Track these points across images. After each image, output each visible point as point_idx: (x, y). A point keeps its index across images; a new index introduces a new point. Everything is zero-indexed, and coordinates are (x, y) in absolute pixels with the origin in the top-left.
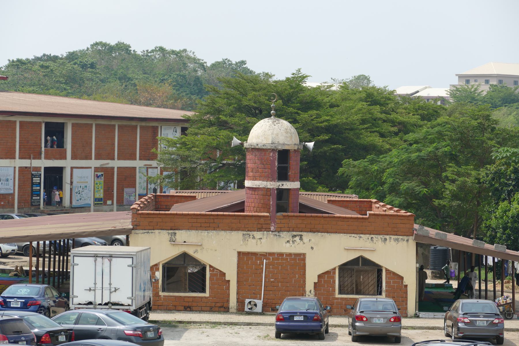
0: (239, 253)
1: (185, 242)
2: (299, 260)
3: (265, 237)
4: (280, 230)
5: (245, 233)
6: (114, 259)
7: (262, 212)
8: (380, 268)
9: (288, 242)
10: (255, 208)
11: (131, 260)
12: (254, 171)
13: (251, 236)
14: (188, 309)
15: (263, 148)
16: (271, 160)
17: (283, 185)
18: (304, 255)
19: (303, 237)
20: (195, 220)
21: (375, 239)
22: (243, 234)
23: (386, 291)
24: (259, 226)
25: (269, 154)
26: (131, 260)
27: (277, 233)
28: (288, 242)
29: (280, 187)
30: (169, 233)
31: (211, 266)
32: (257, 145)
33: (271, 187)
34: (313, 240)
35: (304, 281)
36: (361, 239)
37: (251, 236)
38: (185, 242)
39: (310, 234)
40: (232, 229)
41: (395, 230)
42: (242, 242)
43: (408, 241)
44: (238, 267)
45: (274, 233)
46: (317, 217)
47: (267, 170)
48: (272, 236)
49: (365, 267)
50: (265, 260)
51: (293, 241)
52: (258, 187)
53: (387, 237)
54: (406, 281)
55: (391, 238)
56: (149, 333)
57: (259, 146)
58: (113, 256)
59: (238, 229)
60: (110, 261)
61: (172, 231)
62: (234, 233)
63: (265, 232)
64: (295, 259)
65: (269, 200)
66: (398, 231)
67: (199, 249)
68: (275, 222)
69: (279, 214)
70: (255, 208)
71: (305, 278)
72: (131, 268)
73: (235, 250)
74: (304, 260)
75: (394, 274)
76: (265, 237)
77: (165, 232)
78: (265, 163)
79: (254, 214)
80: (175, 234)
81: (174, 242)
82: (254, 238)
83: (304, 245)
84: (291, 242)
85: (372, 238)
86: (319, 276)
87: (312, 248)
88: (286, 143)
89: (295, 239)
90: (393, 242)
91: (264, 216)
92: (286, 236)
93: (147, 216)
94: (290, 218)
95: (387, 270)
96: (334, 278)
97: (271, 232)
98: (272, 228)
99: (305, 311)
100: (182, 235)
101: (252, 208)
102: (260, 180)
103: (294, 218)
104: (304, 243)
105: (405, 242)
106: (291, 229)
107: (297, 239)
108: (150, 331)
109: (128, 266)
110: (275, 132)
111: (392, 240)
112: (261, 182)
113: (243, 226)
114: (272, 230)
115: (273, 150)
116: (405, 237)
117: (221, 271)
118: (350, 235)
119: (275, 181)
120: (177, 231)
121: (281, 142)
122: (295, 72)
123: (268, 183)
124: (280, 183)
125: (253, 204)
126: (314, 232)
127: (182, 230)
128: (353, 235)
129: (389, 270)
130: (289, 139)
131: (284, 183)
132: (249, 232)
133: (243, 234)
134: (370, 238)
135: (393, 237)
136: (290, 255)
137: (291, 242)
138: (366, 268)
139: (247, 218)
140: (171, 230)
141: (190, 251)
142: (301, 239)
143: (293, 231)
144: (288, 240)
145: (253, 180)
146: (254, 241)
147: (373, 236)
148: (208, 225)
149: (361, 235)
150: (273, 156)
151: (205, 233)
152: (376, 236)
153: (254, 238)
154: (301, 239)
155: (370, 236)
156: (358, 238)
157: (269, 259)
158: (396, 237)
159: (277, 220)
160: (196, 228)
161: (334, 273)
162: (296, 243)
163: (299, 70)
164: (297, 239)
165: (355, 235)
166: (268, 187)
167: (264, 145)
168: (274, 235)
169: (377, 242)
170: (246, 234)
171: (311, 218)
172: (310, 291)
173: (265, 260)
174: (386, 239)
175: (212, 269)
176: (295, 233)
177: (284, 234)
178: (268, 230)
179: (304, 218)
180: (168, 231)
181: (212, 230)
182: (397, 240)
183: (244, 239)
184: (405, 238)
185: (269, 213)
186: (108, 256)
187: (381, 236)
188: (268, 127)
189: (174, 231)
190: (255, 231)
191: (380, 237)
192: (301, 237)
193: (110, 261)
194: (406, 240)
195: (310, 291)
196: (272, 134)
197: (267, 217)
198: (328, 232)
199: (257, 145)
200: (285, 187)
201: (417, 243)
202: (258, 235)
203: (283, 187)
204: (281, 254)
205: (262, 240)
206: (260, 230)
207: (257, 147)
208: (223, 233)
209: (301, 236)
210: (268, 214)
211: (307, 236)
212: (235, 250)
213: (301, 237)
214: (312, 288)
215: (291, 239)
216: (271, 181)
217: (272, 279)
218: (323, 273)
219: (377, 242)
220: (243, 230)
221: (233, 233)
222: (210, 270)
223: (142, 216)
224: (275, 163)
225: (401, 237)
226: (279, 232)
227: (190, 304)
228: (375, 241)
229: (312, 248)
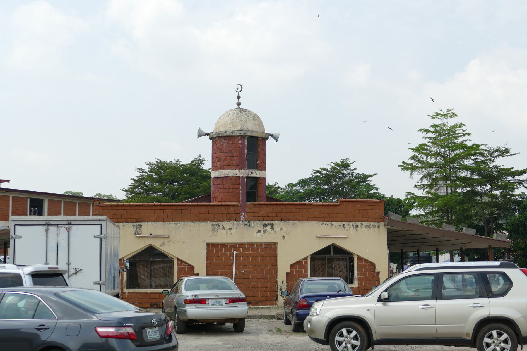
0: (208, 245)
1: (151, 234)
2: (269, 251)
3: (235, 227)
4: (250, 219)
5: (214, 223)
6: (74, 228)
7: (231, 202)
8: (351, 256)
9: (259, 231)
10: (224, 198)
11: (98, 227)
12: (222, 160)
13: (221, 227)
14: (155, 306)
15: (232, 135)
16: (240, 147)
17: (252, 173)
18: (275, 244)
19: (275, 226)
20: (162, 212)
21: (346, 226)
22: (213, 225)
23: (359, 279)
24: (229, 216)
25: (238, 141)
26: (98, 227)
27: (247, 223)
28: (259, 231)
29: (250, 176)
30: (134, 226)
31: (178, 260)
32: (226, 132)
33: (241, 175)
34: (284, 228)
35: (276, 272)
36: (333, 226)
37: (221, 227)
38: (151, 234)
39: (282, 223)
40: (200, 220)
41: (366, 216)
42: (211, 233)
43: (379, 227)
44: (207, 260)
45: (244, 223)
46: (288, 205)
47: (235, 158)
48: (242, 226)
49: (337, 256)
50: (235, 252)
51: (264, 231)
52: (226, 175)
53: (359, 224)
54: (378, 268)
55: (362, 224)
56: (149, 331)
57: (228, 134)
58: (73, 223)
59: (207, 220)
60: (69, 231)
61: (137, 223)
62: (203, 224)
63: (235, 222)
64: (265, 250)
65: (238, 189)
66: (369, 218)
67: (166, 241)
68: (245, 211)
69: (249, 203)
70: (224, 198)
71: (276, 268)
72: (98, 240)
73: (204, 241)
74: (275, 250)
75: (366, 261)
76: (235, 227)
77: (129, 224)
78: (233, 151)
79: (222, 203)
80: (141, 226)
81: (140, 234)
82: (223, 228)
83: (276, 234)
84: (262, 232)
85: (344, 225)
86: (291, 266)
87: (284, 237)
88: (255, 130)
89: (266, 228)
90: (364, 229)
91: (234, 206)
92: (257, 225)
93: (110, 208)
94: (261, 206)
95: (359, 257)
96: (305, 267)
97: (241, 222)
98: (242, 218)
99: (336, 293)
100: (148, 228)
101: (220, 199)
102: (228, 169)
103: (264, 206)
104: (275, 232)
105: (376, 228)
106: (262, 218)
107: (268, 228)
108: (152, 326)
109: (95, 237)
110: (243, 119)
111: (364, 227)
112: (229, 170)
113: (212, 217)
114: (242, 219)
115: (242, 137)
116: (376, 223)
117: (189, 265)
118: (322, 222)
119: (244, 169)
120: (142, 223)
121: (250, 129)
122: (197, 157)
123: (238, 171)
124: (250, 171)
125: (222, 194)
126: (286, 221)
127: (147, 222)
128: (325, 223)
129: (360, 258)
130: (257, 127)
131: (254, 171)
132: (218, 223)
133: (213, 225)
134: (342, 225)
135: (364, 223)
136: (261, 245)
137: (262, 232)
138: (338, 256)
139: (216, 207)
140: (136, 222)
141: (157, 244)
142: (272, 228)
143: (264, 220)
144: (259, 229)
145: (221, 169)
146: (224, 232)
147: (344, 223)
148: (175, 216)
149: (333, 222)
150: (242, 143)
151: (172, 225)
152: (348, 223)
153: (223, 228)
154: (272, 228)
155: (342, 224)
156: (330, 225)
157: (239, 250)
158: (367, 223)
159: (247, 209)
160: (163, 220)
161: (306, 263)
162: (267, 233)
163: (200, 156)
164: (268, 228)
165: (327, 223)
166: (238, 175)
167: (232, 132)
168: (245, 225)
169: (348, 230)
170: (215, 225)
171: (282, 207)
172: (283, 282)
173: (235, 252)
174: (357, 226)
175: (179, 263)
176: (266, 222)
177: (255, 224)
178: (238, 219)
179: (275, 207)
180: (132, 224)
181: (179, 221)
182: (368, 226)
183: (214, 230)
184: (377, 224)
185: (239, 202)
186: (65, 223)
187: (353, 223)
188: (235, 115)
189: (139, 223)
190: (224, 221)
191: (351, 224)
192: (272, 226)
193: (69, 231)
194: (377, 226)
195: (283, 282)
196: (241, 121)
197: (237, 206)
198: (299, 220)
199: (226, 132)
200: (254, 175)
201: (388, 229)
202: (228, 225)
203: (252, 176)
204: (251, 245)
205: (232, 231)
206: (229, 219)
207: (225, 135)
208: (191, 224)
209: (272, 225)
210: (238, 203)
211: (278, 225)
212: (204, 241)
213: (272, 226)
214: (284, 279)
215: (263, 229)
216: (240, 169)
217: (243, 271)
218: (295, 263)
219: (348, 230)
220: (211, 221)
221: (201, 224)
222: (178, 264)
223: (105, 208)
224: (244, 150)
225: (372, 223)
226: (249, 221)
227: (157, 300)
228: (346, 228)
229: (284, 237)
